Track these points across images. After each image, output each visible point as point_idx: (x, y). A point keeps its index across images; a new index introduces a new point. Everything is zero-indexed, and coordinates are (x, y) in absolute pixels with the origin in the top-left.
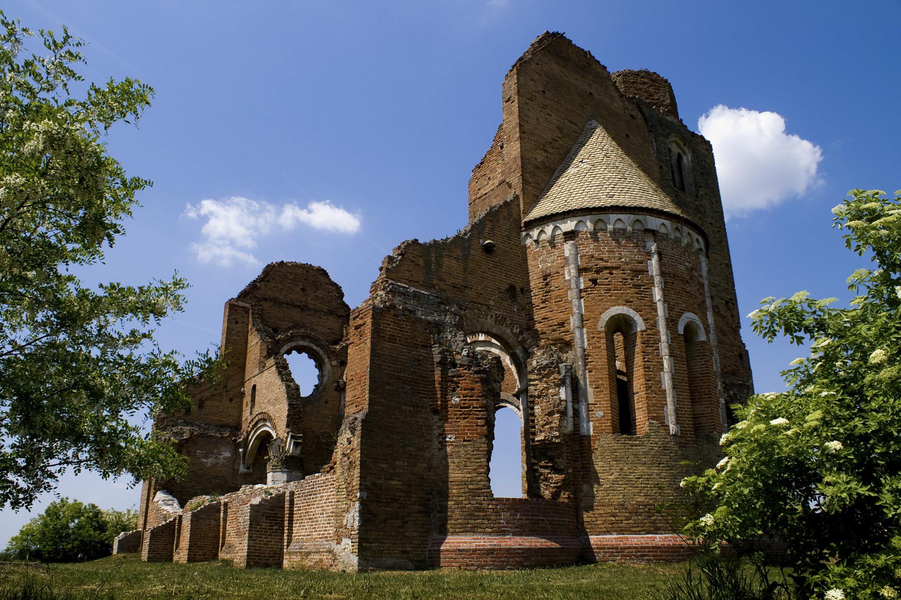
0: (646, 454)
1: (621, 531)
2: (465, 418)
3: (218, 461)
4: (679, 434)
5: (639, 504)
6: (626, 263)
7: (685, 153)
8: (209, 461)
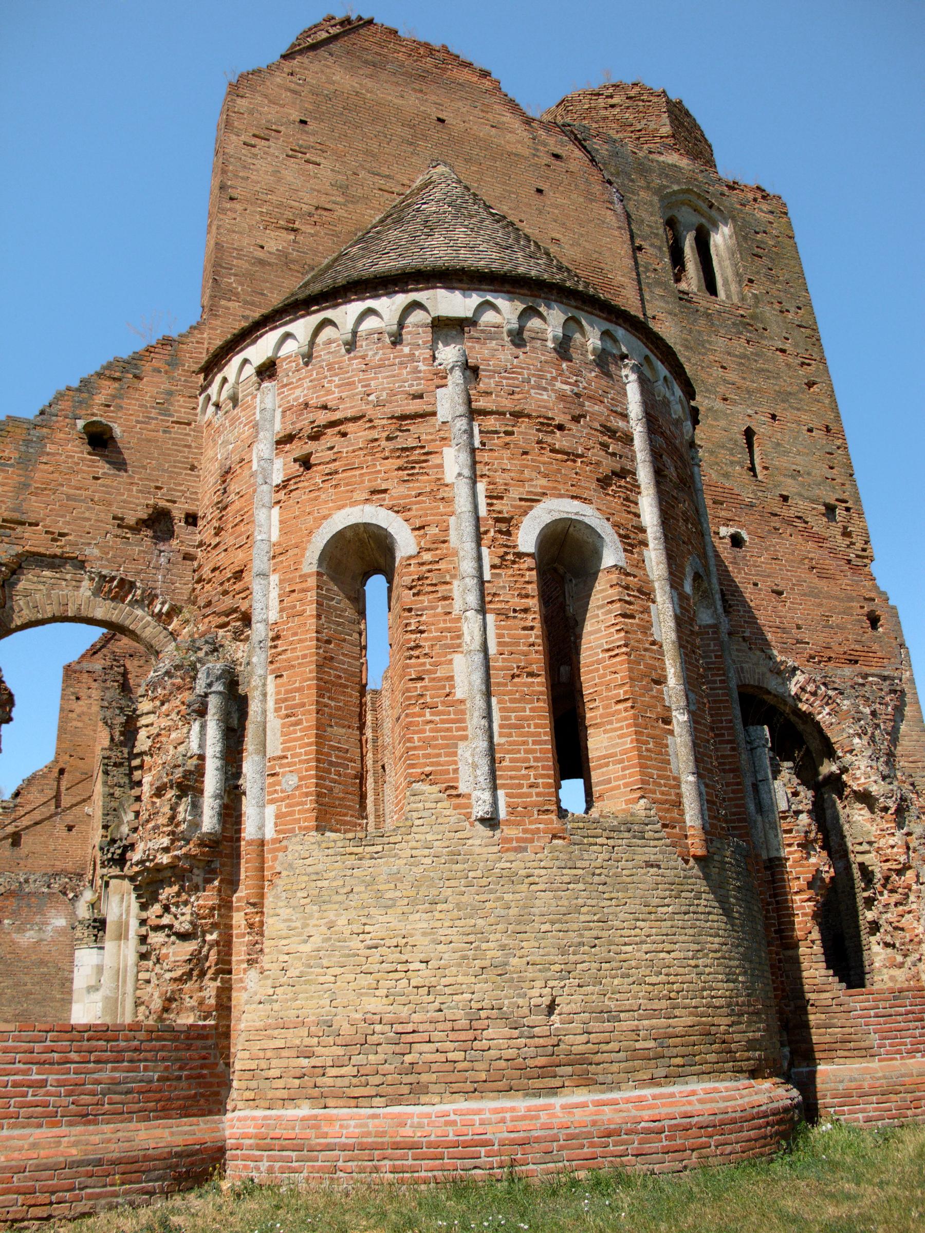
0: (396, 878)
1: (321, 1099)
3: (43, 936)
6: (379, 404)
8: (28, 937)
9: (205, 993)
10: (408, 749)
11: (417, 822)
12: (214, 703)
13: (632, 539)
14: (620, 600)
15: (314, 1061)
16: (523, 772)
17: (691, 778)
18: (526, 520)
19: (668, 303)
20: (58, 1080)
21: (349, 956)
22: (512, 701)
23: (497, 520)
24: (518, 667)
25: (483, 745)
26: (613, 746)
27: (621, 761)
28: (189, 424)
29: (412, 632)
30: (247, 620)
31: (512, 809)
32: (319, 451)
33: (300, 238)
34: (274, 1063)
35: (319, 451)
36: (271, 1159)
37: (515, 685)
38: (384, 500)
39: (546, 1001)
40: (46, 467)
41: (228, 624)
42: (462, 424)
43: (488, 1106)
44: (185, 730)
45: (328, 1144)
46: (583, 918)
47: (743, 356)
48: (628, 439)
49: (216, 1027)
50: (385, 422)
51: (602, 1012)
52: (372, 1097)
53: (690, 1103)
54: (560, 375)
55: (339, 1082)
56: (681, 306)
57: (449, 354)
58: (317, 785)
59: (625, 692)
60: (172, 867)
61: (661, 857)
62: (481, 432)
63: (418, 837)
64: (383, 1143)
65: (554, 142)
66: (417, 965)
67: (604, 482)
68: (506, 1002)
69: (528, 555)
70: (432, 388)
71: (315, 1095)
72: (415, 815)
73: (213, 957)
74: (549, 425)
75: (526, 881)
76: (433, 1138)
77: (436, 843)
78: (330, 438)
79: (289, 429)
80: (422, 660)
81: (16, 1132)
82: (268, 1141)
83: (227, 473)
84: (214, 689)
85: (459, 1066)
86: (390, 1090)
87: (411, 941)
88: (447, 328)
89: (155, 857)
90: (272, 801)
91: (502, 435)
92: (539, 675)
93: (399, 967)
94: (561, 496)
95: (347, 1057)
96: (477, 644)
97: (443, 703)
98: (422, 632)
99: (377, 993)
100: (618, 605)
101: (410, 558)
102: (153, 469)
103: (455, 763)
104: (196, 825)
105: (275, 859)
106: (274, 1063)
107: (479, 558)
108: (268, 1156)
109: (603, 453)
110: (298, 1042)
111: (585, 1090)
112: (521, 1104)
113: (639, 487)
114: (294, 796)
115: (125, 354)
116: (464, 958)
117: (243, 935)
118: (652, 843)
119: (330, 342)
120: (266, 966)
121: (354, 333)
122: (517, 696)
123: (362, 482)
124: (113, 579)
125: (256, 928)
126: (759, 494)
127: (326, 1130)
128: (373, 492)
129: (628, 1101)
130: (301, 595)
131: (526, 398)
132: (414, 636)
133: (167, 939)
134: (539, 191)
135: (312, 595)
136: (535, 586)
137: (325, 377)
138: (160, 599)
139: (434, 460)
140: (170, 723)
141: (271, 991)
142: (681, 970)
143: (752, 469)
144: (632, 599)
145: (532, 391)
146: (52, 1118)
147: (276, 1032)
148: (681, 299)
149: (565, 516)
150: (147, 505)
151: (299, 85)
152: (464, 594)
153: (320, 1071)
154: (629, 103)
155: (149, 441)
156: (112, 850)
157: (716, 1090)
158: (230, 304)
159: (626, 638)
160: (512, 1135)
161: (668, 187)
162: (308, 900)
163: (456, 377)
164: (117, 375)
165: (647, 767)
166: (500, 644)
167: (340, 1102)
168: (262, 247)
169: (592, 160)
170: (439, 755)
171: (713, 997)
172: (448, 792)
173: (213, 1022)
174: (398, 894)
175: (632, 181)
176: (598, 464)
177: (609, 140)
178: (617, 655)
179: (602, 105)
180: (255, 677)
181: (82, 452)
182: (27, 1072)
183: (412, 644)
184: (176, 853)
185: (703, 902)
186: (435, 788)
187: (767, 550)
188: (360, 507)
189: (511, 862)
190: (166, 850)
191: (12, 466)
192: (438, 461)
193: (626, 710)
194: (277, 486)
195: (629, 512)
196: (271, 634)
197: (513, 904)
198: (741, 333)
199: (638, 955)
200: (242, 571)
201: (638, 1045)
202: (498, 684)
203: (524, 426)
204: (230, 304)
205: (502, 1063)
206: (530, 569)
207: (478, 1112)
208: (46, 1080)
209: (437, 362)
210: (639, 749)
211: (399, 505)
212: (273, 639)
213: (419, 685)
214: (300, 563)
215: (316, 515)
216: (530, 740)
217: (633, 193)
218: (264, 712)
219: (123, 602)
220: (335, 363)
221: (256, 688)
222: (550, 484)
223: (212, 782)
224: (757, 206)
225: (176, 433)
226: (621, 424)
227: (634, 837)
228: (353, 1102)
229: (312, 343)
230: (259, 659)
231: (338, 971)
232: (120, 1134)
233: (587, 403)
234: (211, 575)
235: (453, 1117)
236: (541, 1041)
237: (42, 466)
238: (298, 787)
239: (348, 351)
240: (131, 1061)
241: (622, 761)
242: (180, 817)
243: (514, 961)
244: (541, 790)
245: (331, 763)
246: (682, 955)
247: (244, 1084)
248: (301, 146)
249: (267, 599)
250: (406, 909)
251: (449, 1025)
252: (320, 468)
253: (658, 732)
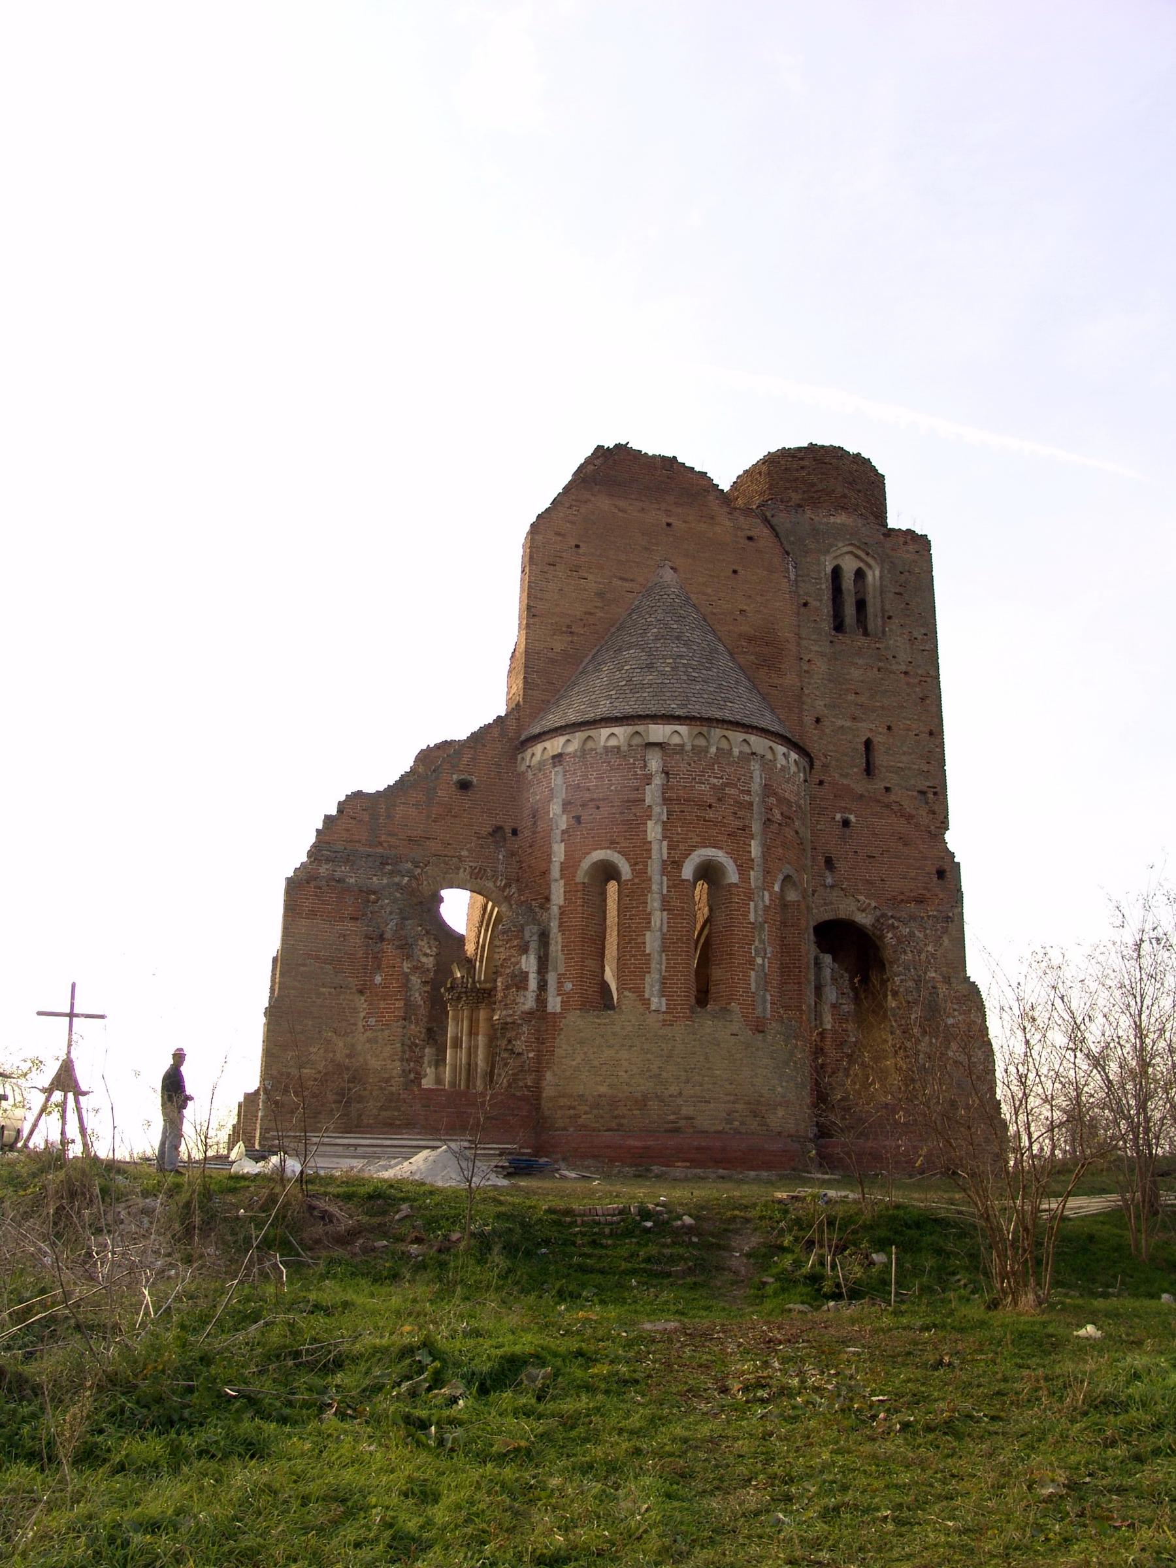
4: (664, 1009)
7: (870, 567)
134: (735, 572)
169: (777, 536)
223: (533, 984)
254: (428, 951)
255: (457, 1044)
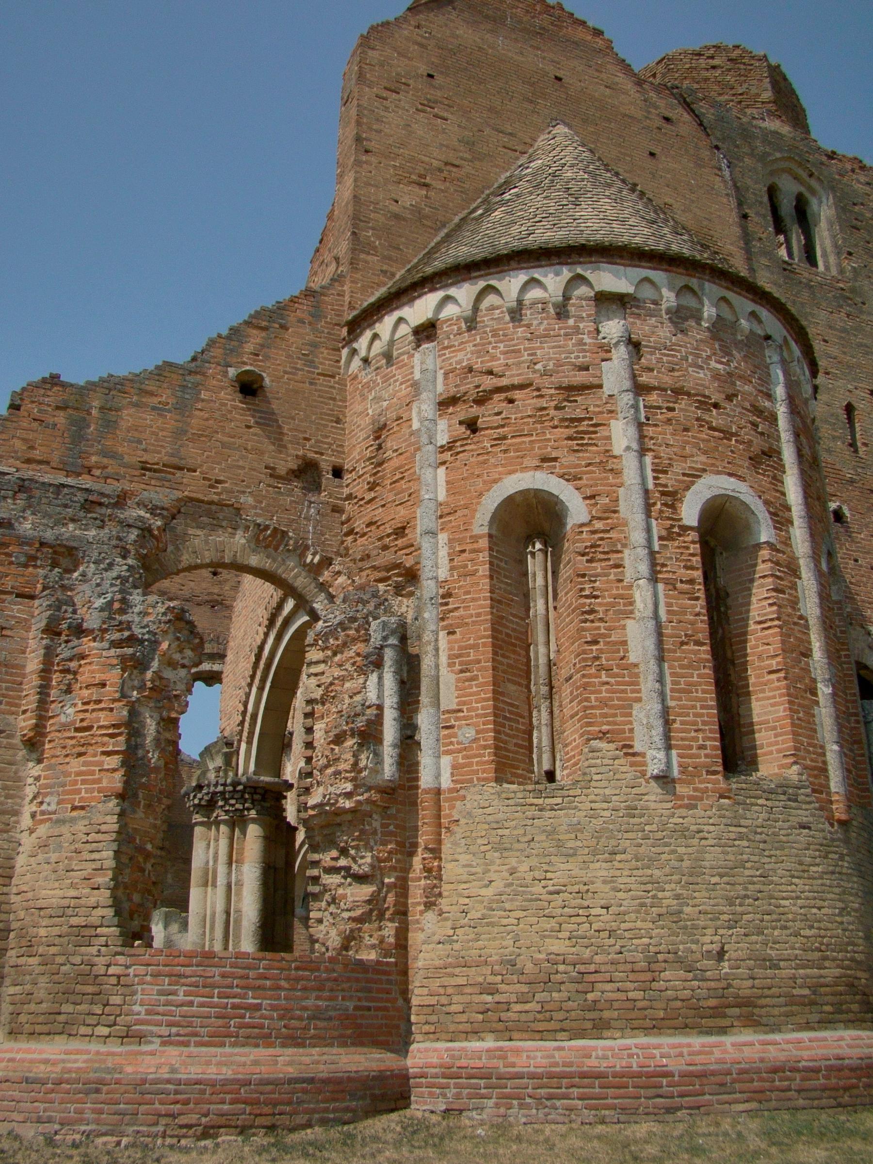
0: (577, 829)
1: (506, 1031)
2: (80, 755)
5: (554, 960)
6: (546, 373)
7: (813, 192)
9: (385, 932)
10: (586, 708)
11: (595, 777)
12: (389, 655)
13: (780, 517)
14: (772, 575)
15: (498, 998)
16: (693, 734)
17: (836, 747)
18: (689, 494)
19: (772, 273)
20: (271, 1005)
21: (531, 900)
22: (682, 667)
23: (663, 494)
24: (686, 635)
25: (656, 707)
26: (765, 713)
27: (774, 728)
28: (333, 377)
29: (587, 597)
30: (412, 576)
31: (684, 769)
32: (486, 415)
33: (432, 194)
34: (455, 999)
35: (486, 415)
36: (457, 1086)
37: (684, 652)
38: (555, 468)
39: (716, 947)
40: (202, 414)
41: (388, 578)
42: (627, 398)
43: (667, 1041)
44: (361, 681)
45: (517, 1073)
46: (747, 872)
47: (844, 330)
48: (773, 419)
49: (396, 964)
50: (553, 391)
51: (764, 960)
52: (556, 1031)
53: (840, 1047)
54: (715, 354)
55: (523, 1017)
56: (786, 277)
57: (613, 328)
58: (495, 738)
59: (778, 663)
60: (353, 811)
61: (811, 819)
62: (645, 407)
63: (596, 791)
64: (571, 1072)
65: (665, 105)
66: (599, 911)
67: (755, 461)
68: (681, 947)
69: (691, 528)
70: (597, 361)
71: (500, 1028)
72: (593, 770)
73: (391, 899)
74: (705, 403)
75: (697, 836)
76: (618, 1069)
77: (614, 798)
78: (497, 402)
79: (453, 391)
80: (597, 624)
81: (236, 1050)
82: (455, 1069)
83: (379, 431)
84: (390, 642)
85: (640, 1004)
86: (574, 1024)
87: (591, 887)
88: (607, 301)
89: (337, 801)
90: (447, 753)
91: (664, 411)
92: (705, 644)
93: (581, 912)
94: (719, 473)
95: (531, 995)
96: (649, 612)
97: (618, 666)
98: (596, 597)
99: (560, 935)
100: (770, 580)
101: (582, 525)
102: (301, 421)
103: (631, 723)
104: (377, 770)
105: (452, 807)
106: (455, 999)
107: (648, 530)
108: (455, 1084)
109: (753, 432)
110: (480, 979)
111: (751, 1030)
112: (697, 1041)
113: (783, 466)
114: (471, 748)
115: (270, 304)
116: (642, 905)
117: (419, 879)
118: (804, 806)
119: (492, 308)
120: (445, 908)
121: (520, 302)
122: (685, 662)
123: (533, 449)
124: (267, 527)
125: (433, 873)
126: (859, 470)
127: (513, 1060)
128: (544, 460)
129: (788, 1042)
130: (473, 556)
131: (684, 376)
132: (588, 601)
133: (343, 881)
134: (652, 154)
135: (484, 556)
136: (699, 558)
137: (490, 343)
138: (312, 550)
139: (602, 432)
140: (343, 673)
141: (451, 932)
142: (830, 925)
143: (853, 445)
144: (782, 575)
145: (690, 369)
146: (265, 1039)
147: (457, 971)
148: (785, 270)
149: (723, 492)
150: (297, 456)
151: (425, 38)
152: (635, 563)
153: (505, 1006)
154: (729, 65)
155: (297, 392)
156: (199, 796)
157: (859, 1038)
158: (369, 258)
159: (779, 612)
160: (691, 1068)
161: (769, 154)
162: (489, 847)
163: (621, 353)
164: (264, 324)
165: (799, 735)
166: (669, 612)
167: (525, 1035)
168: (397, 202)
169: (701, 124)
170: (615, 715)
171: (855, 952)
172: (625, 750)
173: (393, 960)
174: (579, 843)
175: (737, 147)
176: (750, 442)
177: (714, 104)
178: (769, 628)
179: (704, 66)
180: (428, 633)
181: (234, 400)
182: (244, 996)
183: (587, 608)
184: (359, 798)
185: (846, 864)
186: (612, 746)
187: (867, 526)
188: (531, 473)
189: (683, 818)
190: (348, 795)
191: (169, 411)
192: (606, 434)
193: (778, 680)
194: (442, 447)
195: (777, 491)
196: (441, 591)
197: (685, 857)
198: (841, 307)
199: (794, 909)
200: (404, 528)
201: (795, 992)
202: (669, 651)
203: (683, 402)
204: (369, 258)
205: (679, 1004)
206: (693, 542)
207: (658, 1047)
208: (261, 1004)
209: (601, 335)
210: (792, 718)
211: (569, 474)
212: (443, 597)
213: (594, 648)
214: (471, 524)
215: (486, 478)
216: (698, 704)
217: (738, 159)
218: (437, 666)
219: (276, 549)
220: (500, 329)
221: (429, 642)
222: (710, 461)
223: (390, 732)
224: (855, 176)
225: (322, 385)
226: (767, 404)
227: (789, 800)
228: (537, 1036)
229: (476, 309)
230: (429, 614)
231: (521, 914)
232: (325, 1057)
233: (738, 383)
234: (366, 530)
235: (634, 1050)
236: (712, 984)
237: (197, 413)
238: (475, 740)
239: (513, 319)
240: (332, 990)
241: (775, 728)
242: (362, 764)
243: (687, 910)
244: (708, 751)
245: (505, 718)
246: (830, 911)
247: (422, 1019)
248: (429, 100)
249: (437, 557)
250: (586, 858)
251: (629, 967)
252: (487, 432)
253: (806, 702)
254: (177, 656)
255: (208, 881)
